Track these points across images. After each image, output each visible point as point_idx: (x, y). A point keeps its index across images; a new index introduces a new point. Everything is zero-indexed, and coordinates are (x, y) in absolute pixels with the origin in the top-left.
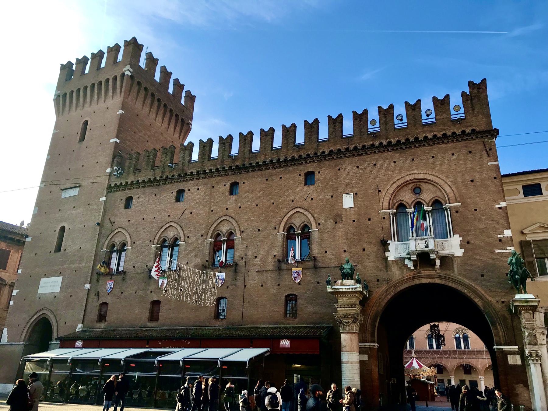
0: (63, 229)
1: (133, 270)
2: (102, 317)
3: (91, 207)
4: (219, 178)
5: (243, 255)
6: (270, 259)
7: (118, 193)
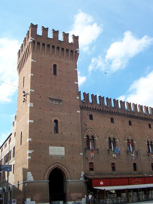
0: (56, 121)
1: (100, 149)
2: (91, 169)
3: (72, 114)
4: (125, 117)
5: (138, 149)
6: (145, 151)
7: (85, 111)
